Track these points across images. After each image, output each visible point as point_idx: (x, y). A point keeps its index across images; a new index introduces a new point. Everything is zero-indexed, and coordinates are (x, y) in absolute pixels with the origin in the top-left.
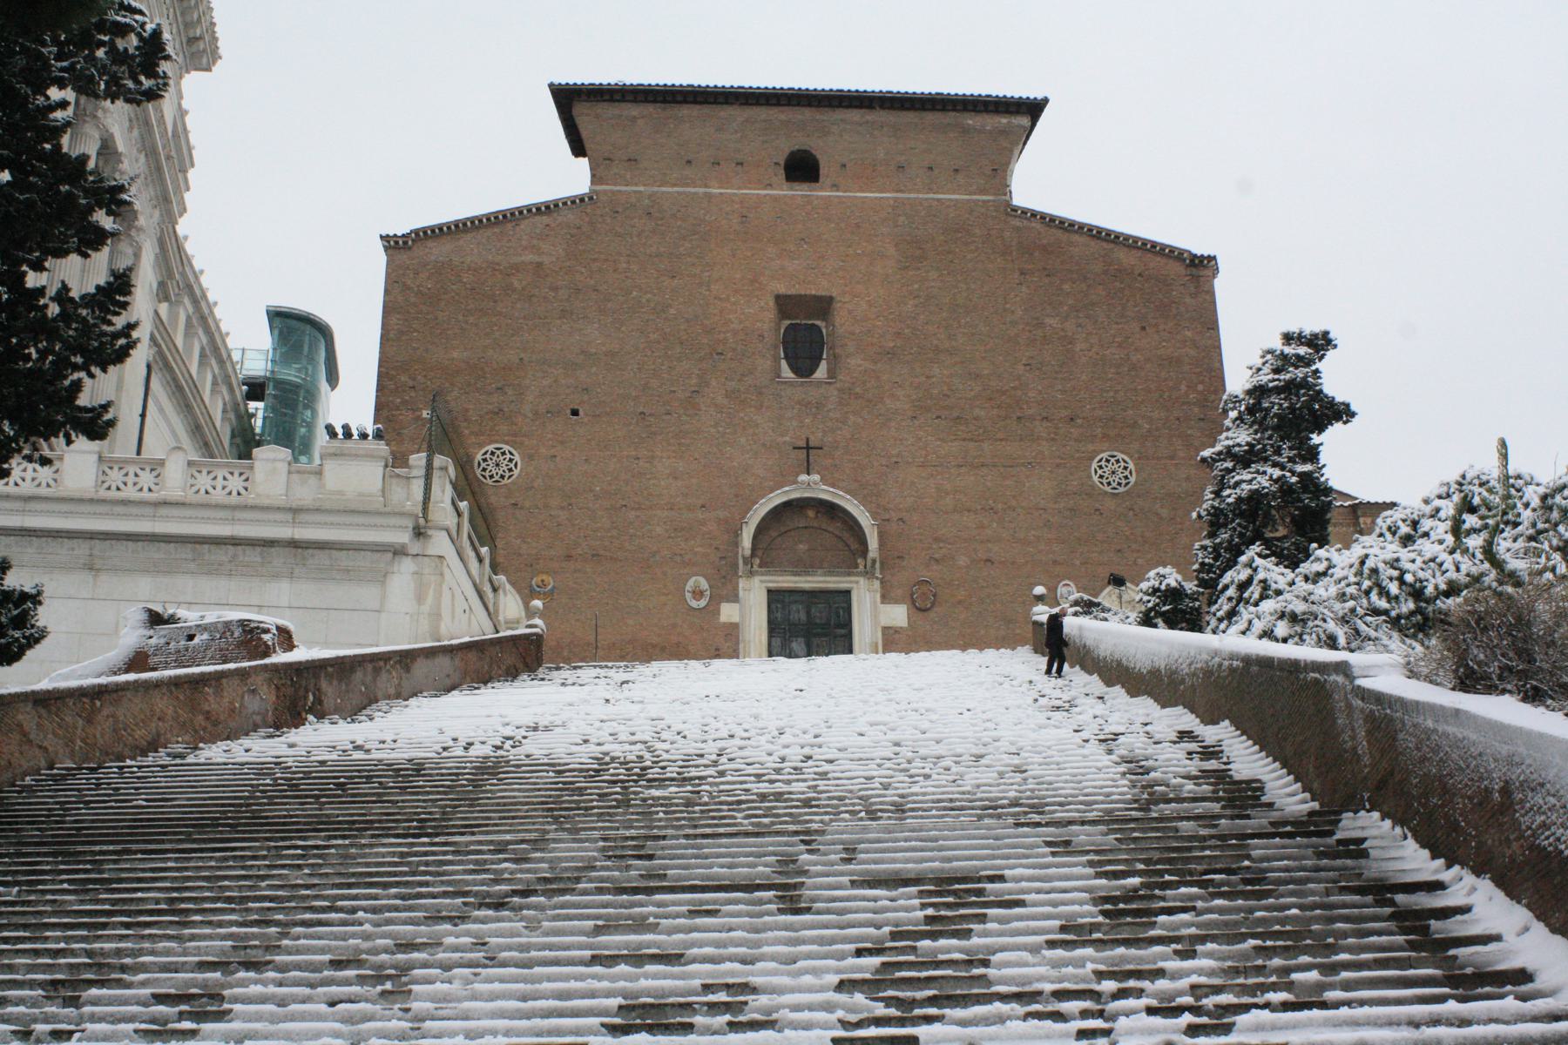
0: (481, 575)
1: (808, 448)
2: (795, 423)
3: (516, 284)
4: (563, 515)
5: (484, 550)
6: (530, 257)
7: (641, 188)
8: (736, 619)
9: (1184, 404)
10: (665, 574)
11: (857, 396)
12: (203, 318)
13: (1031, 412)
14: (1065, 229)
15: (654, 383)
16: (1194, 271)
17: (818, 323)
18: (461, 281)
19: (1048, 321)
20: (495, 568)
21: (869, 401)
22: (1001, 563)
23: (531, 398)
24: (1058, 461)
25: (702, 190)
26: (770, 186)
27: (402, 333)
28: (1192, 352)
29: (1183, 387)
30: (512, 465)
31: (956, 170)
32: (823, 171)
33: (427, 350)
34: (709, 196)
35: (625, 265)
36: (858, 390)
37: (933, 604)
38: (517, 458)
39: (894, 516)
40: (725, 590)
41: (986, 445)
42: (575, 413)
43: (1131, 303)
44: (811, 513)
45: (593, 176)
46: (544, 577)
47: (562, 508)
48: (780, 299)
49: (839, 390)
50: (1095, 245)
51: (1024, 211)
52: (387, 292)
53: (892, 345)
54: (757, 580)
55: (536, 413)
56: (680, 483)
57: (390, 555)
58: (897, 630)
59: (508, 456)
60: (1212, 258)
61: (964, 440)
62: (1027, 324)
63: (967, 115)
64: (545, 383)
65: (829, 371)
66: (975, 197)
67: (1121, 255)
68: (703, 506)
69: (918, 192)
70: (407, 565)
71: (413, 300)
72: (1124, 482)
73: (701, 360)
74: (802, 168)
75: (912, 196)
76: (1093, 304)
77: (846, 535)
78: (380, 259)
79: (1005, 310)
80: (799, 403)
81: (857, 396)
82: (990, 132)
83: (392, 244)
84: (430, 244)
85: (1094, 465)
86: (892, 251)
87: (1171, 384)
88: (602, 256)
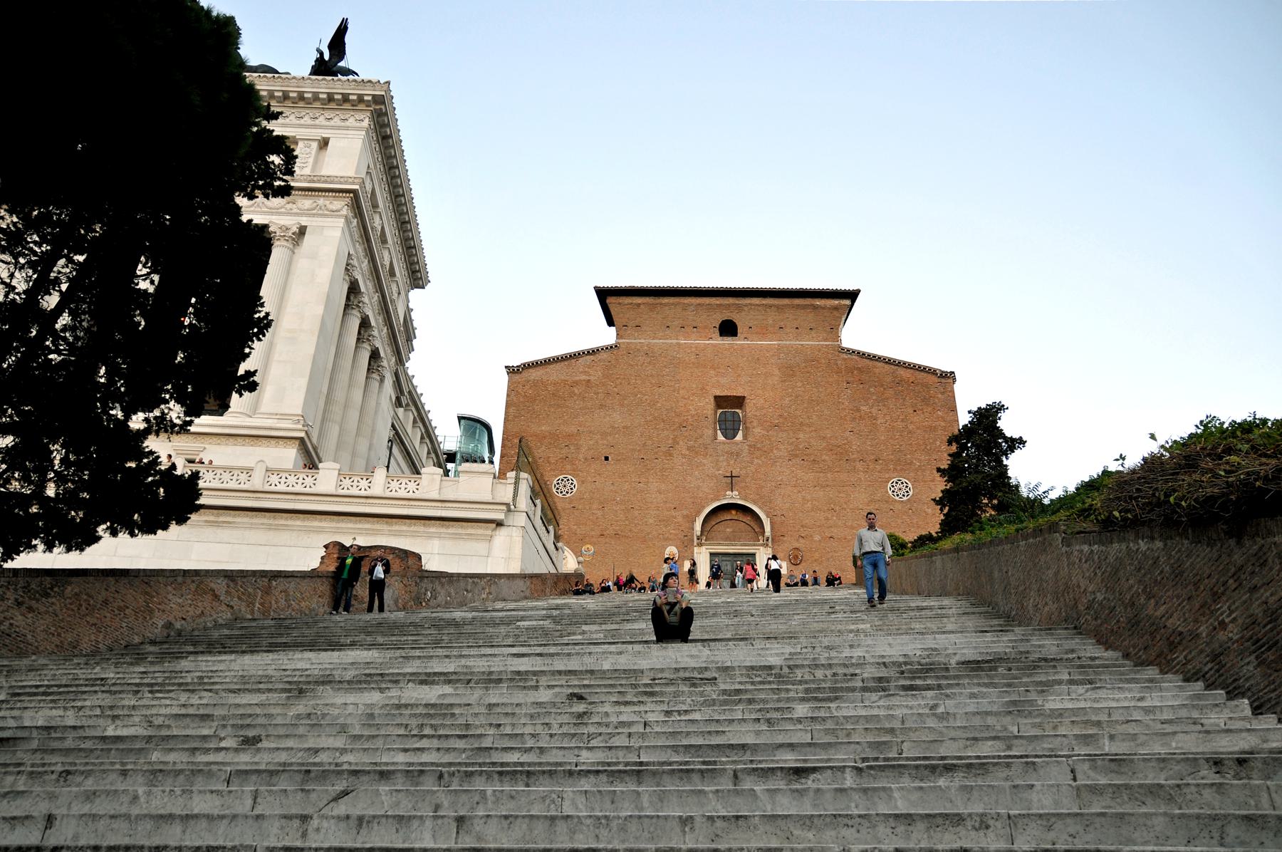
1: (732, 477)
2: (725, 464)
3: (576, 391)
4: (599, 513)
5: (551, 528)
6: (584, 377)
7: (643, 341)
10: (654, 544)
11: (759, 449)
12: (422, 418)
13: (855, 456)
14: (871, 359)
16: (943, 380)
20: (557, 538)
22: (838, 539)
25: (674, 341)
27: (515, 417)
28: (943, 424)
29: (938, 443)
33: (528, 426)
34: (678, 344)
36: (759, 446)
37: (801, 561)
38: (575, 482)
42: (607, 459)
44: (734, 512)
45: (618, 334)
46: (589, 546)
48: (716, 397)
49: (750, 446)
50: (886, 366)
52: (508, 395)
54: (704, 547)
56: (662, 496)
57: (494, 525)
59: (571, 481)
61: (817, 472)
62: (851, 410)
64: (591, 443)
66: (822, 343)
67: (902, 372)
69: (790, 340)
70: (503, 532)
71: (521, 400)
72: (906, 494)
74: (728, 329)
75: (788, 343)
77: (752, 524)
78: (506, 377)
80: (726, 453)
81: (759, 449)
82: (829, 309)
83: (512, 371)
84: (531, 370)
85: (889, 485)
86: (777, 372)
87: (931, 441)
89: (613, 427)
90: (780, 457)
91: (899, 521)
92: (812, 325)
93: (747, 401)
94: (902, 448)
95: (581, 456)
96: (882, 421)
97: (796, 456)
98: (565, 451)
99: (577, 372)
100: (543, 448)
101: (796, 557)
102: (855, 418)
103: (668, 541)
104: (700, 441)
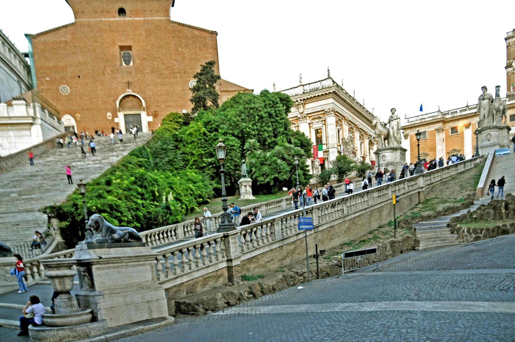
3: (62, 46)
4: (80, 101)
6: (63, 39)
7: (86, 20)
11: (138, 70)
15: (95, 69)
23: (69, 73)
25: (99, 19)
26: (115, 17)
32: (127, 12)
34: (101, 21)
39: (148, 97)
40: (115, 116)
41: (167, 80)
42: (79, 77)
49: (135, 68)
50: (189, 29)
51: (173, 21)
55: (71, 78)
58: (150, 122)
65: (133, 63)
76: (189, 44)
81: (138, 70)
85: (190, 83)
86: (144, 33)
89: (79, 62)
90: (147, 73)
92: (158, 9)
93: (133, 48)
95: (69, 76)
96: (187, 55)
98: (62, 74)
99: (60, 37)
101: (155, 114)
103: (108, 110)
104: (115, 67)
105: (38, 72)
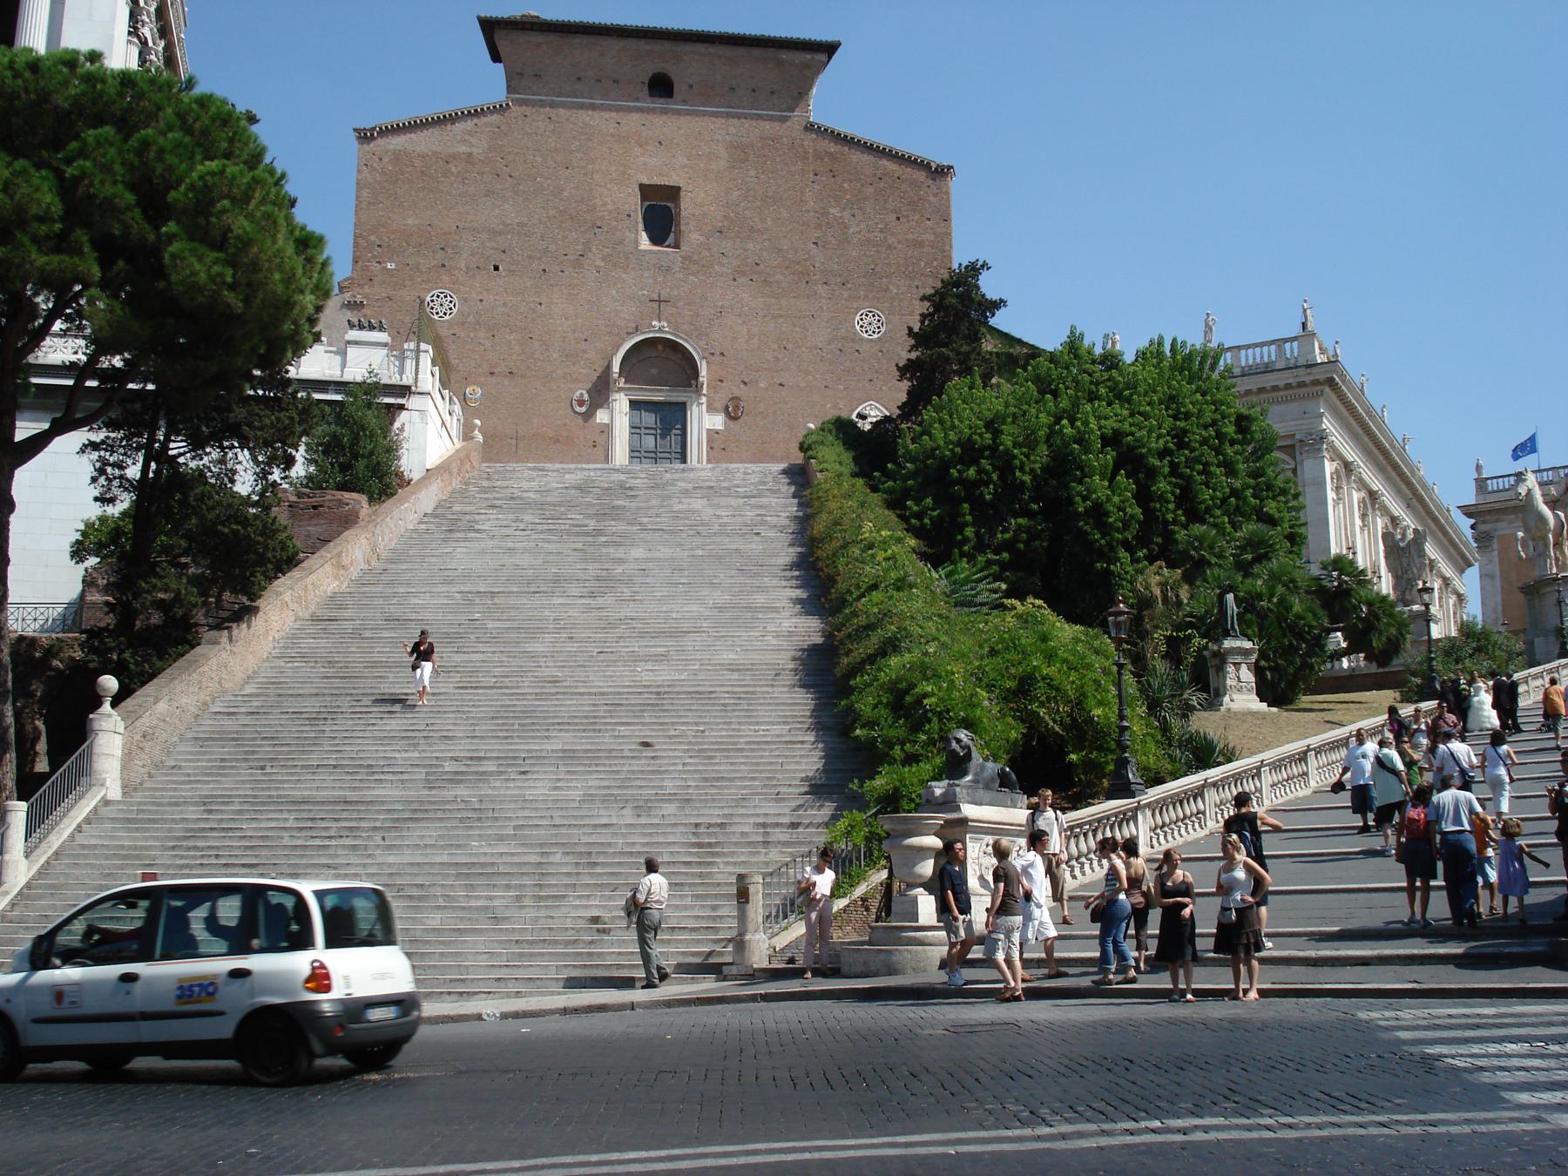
0: (444, 409)
2: (651, 281)
3: (453, 169)
4: (488, 344)
6: (463, 149)
7: (544, 98)
8: (606, 421)
9: (922, 275)
11: (695, 262)
15: (553, 248)
17: (669, 204)
18: (412, 166)
19: (832, 211)
21: (703, 266)
24: (832, 314)
26: (637, 100)
28: (932, 238)
29: (923, 264)
30: (452, 305)
31: (772, 92)
32: (675, 90)
35: (531, 157)
36: (696, 257)
41: (783, 302)
42: (496, 268)
43: (891, 199)
45: (509, 87)
46: (474, 387)
47: (488, 338)
48: (642, 187)
49: (684, 258)
53: (720, 224)
55: (468, 268)
59: (449, 298)
60: (950, 167)
62: (817, 212)
63: (782, 51)
68: (586, 340)
72: (877, 330)
73: (585, 231)
74: (661, 86)
75: (740, 111)
76: (865, 199)
79: (802, 201)
85: (858, 318)
86: (724, 154)
88: (516, 150)
89: (504, 224)
91: (866, 367)
93: (682, 194)
94: (878, 269)
95: (462, 265)
97: (743, 273)
100: (411, 250)
101: (737, 407)
102: (820, 225)
104: (620, 248)
105: (363, 243)
